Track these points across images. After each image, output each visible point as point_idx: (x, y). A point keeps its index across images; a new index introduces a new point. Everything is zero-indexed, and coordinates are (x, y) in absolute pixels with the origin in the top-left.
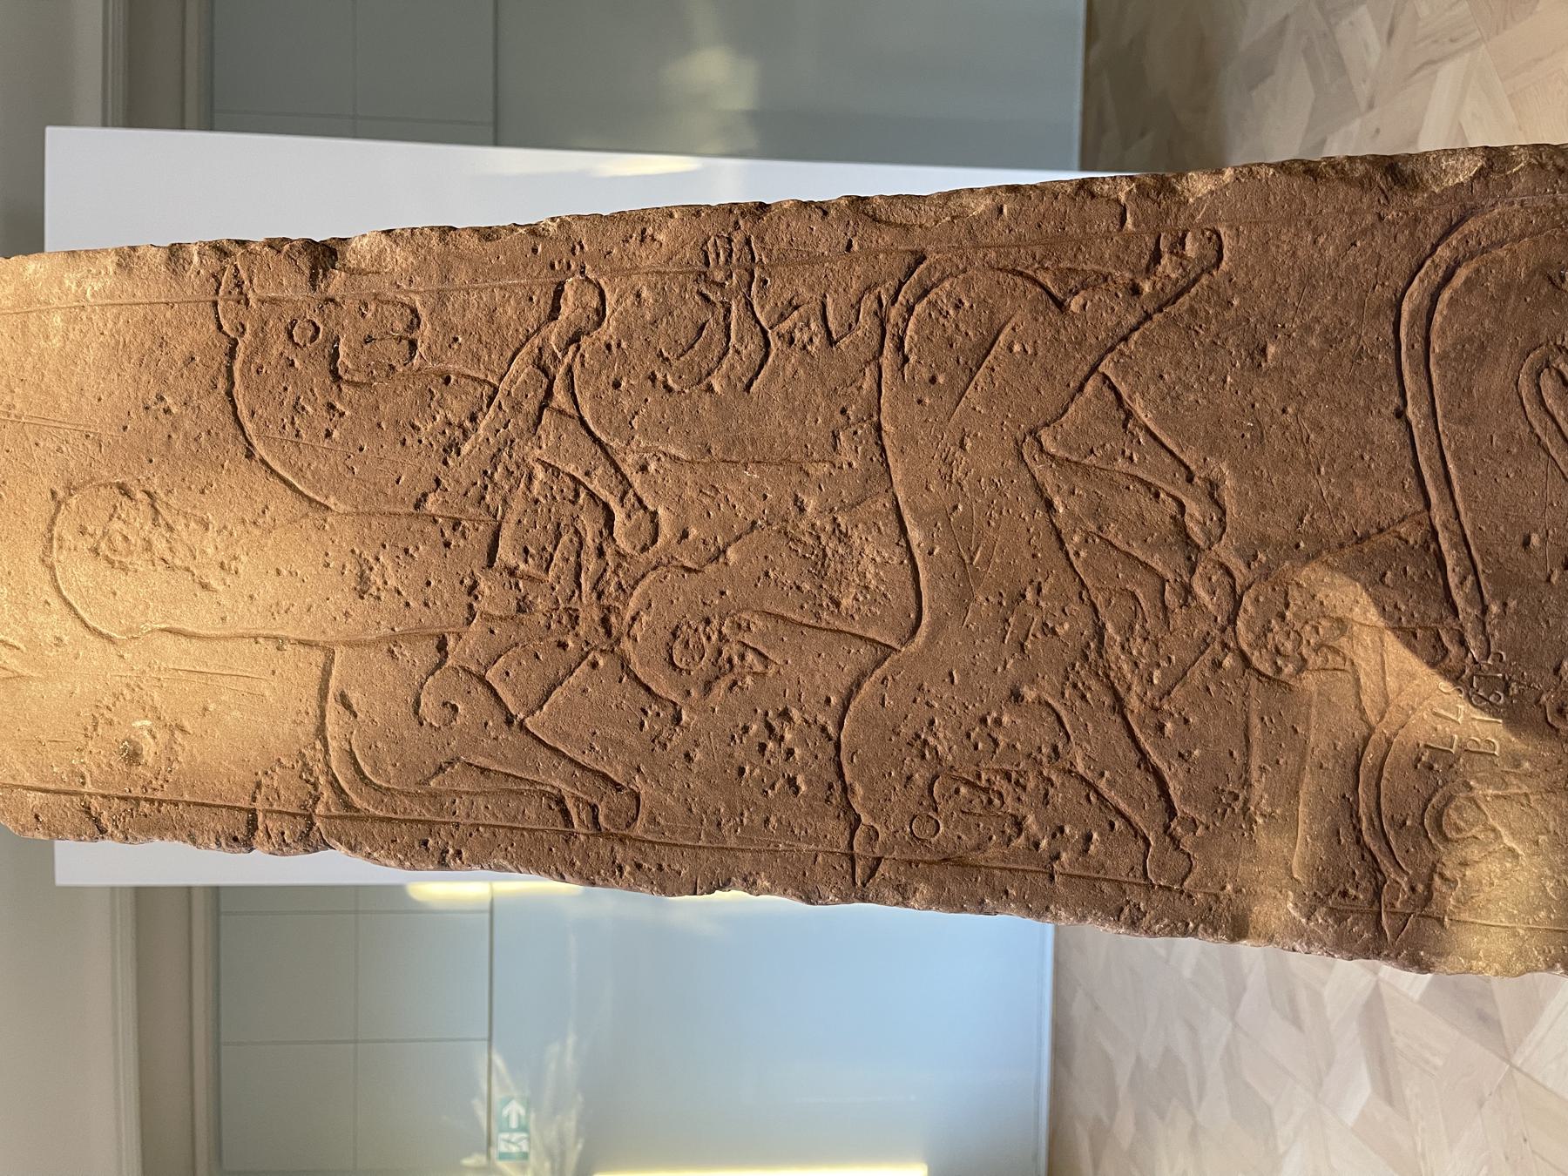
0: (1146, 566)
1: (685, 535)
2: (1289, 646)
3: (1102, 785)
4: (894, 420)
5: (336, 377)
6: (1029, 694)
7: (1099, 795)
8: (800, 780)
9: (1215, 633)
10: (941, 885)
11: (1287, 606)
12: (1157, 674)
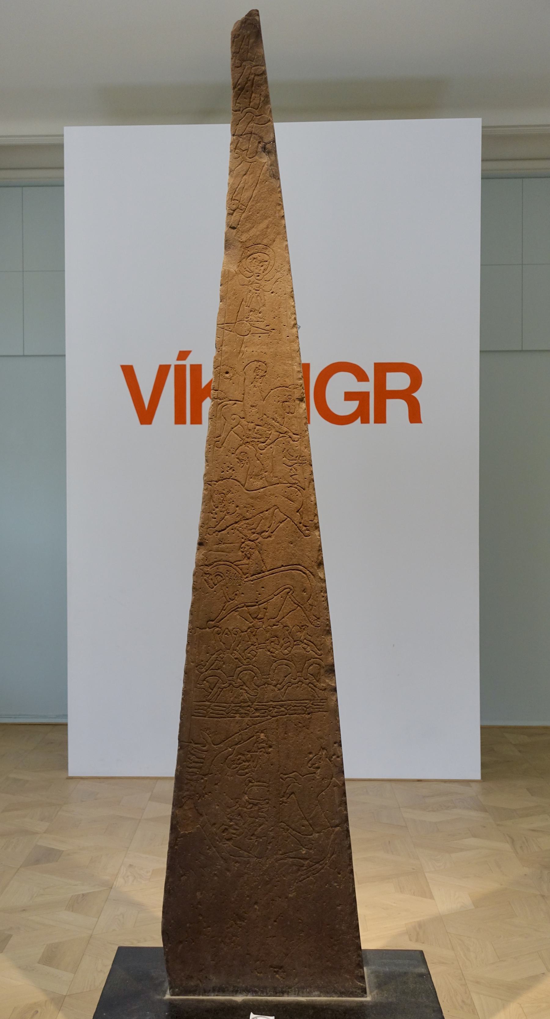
0: (258, 526)
1: (261, 454)
2: (246, 549)
3: (223, 520)
4: (279, 486)
5: (283, 402)
6: (237, 509)
7: (222, 520)
8: (223, 473)
9: (248, 538)
10: (207, 495)
11: (252, 549)
12: (241, 529)
